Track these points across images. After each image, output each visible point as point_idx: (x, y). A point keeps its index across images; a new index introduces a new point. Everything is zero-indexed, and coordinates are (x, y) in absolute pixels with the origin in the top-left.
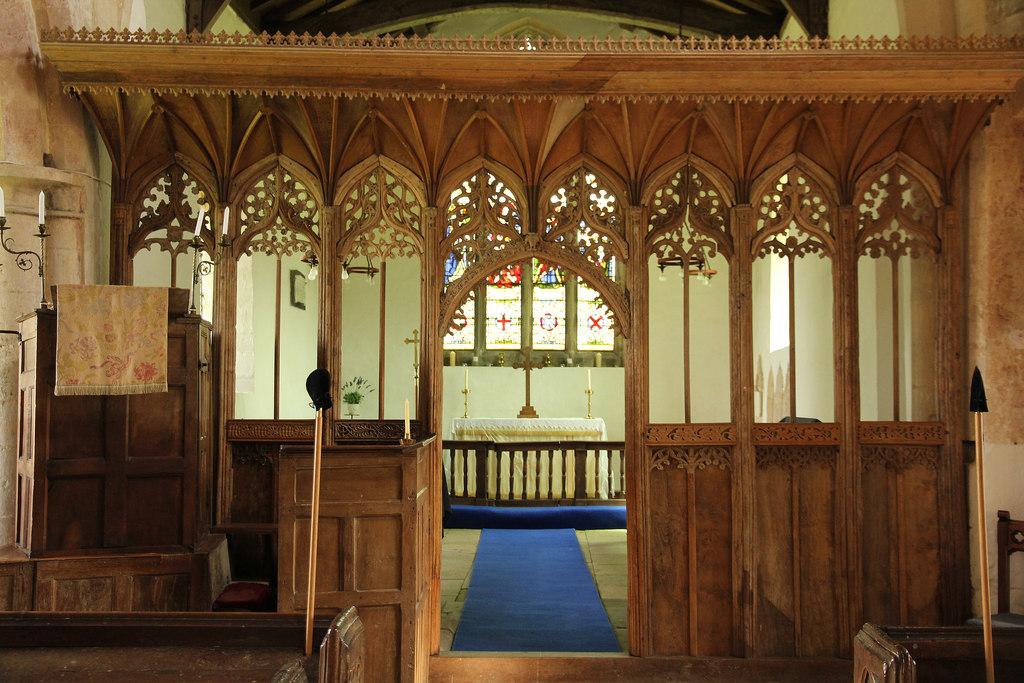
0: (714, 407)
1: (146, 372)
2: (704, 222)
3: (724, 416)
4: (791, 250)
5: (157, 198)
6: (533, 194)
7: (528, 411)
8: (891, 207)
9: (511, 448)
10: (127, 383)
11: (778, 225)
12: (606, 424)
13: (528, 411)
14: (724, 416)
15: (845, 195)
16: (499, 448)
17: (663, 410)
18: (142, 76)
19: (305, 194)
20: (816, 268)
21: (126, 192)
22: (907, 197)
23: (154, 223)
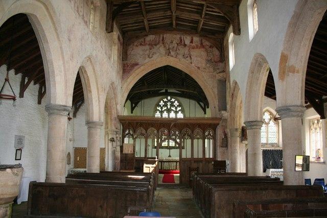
0: (189, 156)
1: (131, 151)
2: (188, 135)
3: (190, 157)
4: (198, 139)
5: (127, 132)
6: (169, 132)
7: (170, 156)
8: (209, 134)
9: (166, 162)
10: (129, 152)
11: (196, 136)
12: (178, 158)
13: (170, 156)
14: (190, 157)
15: (204, 133)
16: (164, 162)
17: (184, 156)
18: (128, 120)
19: (144, 131)
20: (201, 141)
21: (124, 131)
22: (211, 133)
23: (126, 135)
